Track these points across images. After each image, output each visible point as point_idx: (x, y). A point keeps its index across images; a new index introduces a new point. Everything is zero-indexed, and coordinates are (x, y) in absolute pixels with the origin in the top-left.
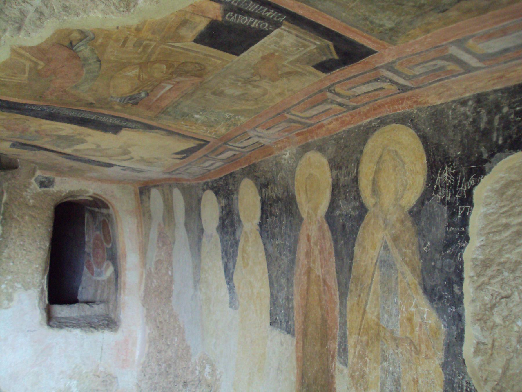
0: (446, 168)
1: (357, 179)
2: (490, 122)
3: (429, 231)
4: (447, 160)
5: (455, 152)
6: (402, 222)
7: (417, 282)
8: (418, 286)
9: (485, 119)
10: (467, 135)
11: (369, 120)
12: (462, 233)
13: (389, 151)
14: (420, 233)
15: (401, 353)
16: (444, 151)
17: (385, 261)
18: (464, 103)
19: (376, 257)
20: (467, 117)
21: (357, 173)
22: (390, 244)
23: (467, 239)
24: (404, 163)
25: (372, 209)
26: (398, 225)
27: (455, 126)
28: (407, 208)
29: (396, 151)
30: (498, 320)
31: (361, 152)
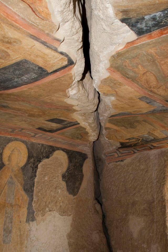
0: (32, 158)
1: (2, 154)
2: (43, 151)
3: (27, 174)
4: (33, 157)
5: (35, 155)
6: (19, 171)
7: (22, 188)
8: (22, 189)
9: (43, 150)
10: (38, 152)
11: (11, 137)
12: (35, 175)
13: (17, 149)
14: (24, 174)
15: (14, 209)
16: (33, 154)
17: (10, 182)
18: (39, 144)
19: (7, 181)
20: (39, 148)
21: (2, 152)
22: (13, 177)
23: (36, 176)
24: (21, 154)
25: (7, 165)
26: (17, 171)
27: (36, 149)
28: (21, 167)
29: (19, 150)
30: (40, 194)
31: (5, 146)
